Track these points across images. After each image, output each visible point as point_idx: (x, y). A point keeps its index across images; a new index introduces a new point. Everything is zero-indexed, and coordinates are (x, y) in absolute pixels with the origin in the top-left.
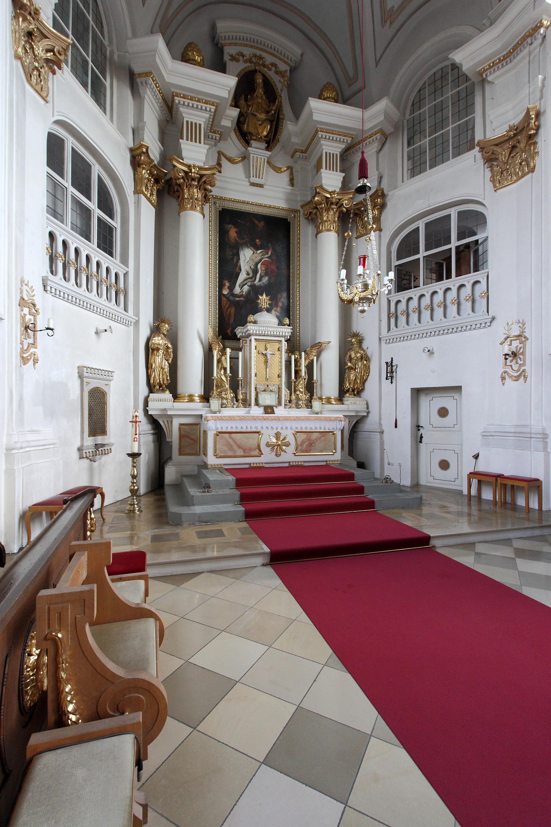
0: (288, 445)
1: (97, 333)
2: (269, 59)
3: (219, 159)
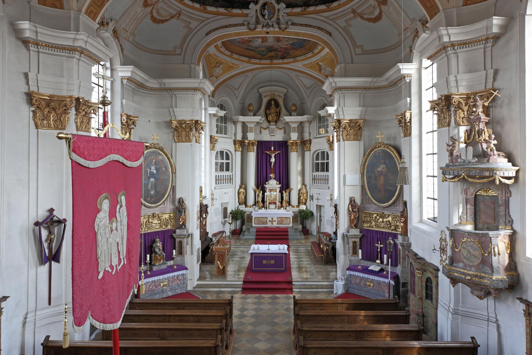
0: (275, 221)
1: (225, 193)
2: (277, 93)
3: (261, 129)
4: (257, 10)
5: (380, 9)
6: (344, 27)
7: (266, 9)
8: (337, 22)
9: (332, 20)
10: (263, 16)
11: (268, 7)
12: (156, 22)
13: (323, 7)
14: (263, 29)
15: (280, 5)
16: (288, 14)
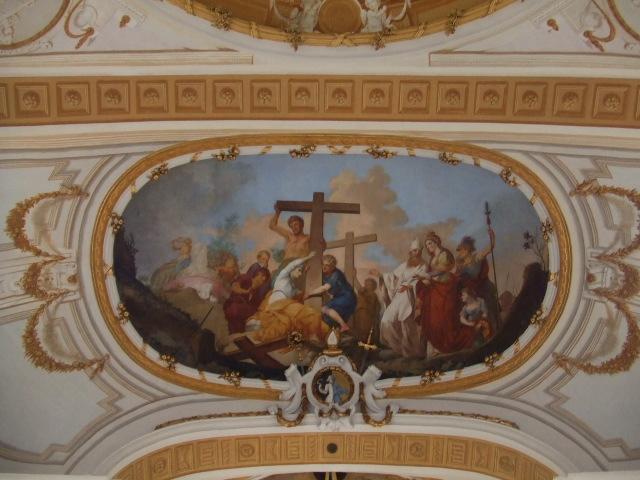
4: (304, 386)
5: (628, 316)
6: (549, 405)
7: (328, 383)
8: (522, 397)
9: (508, 396)
10: (322, 397)
11: (334, 380)
12: (34, 356)
13: (479, 369)
14: (319, 424)
15: (366, 374)
16: (390, 393)
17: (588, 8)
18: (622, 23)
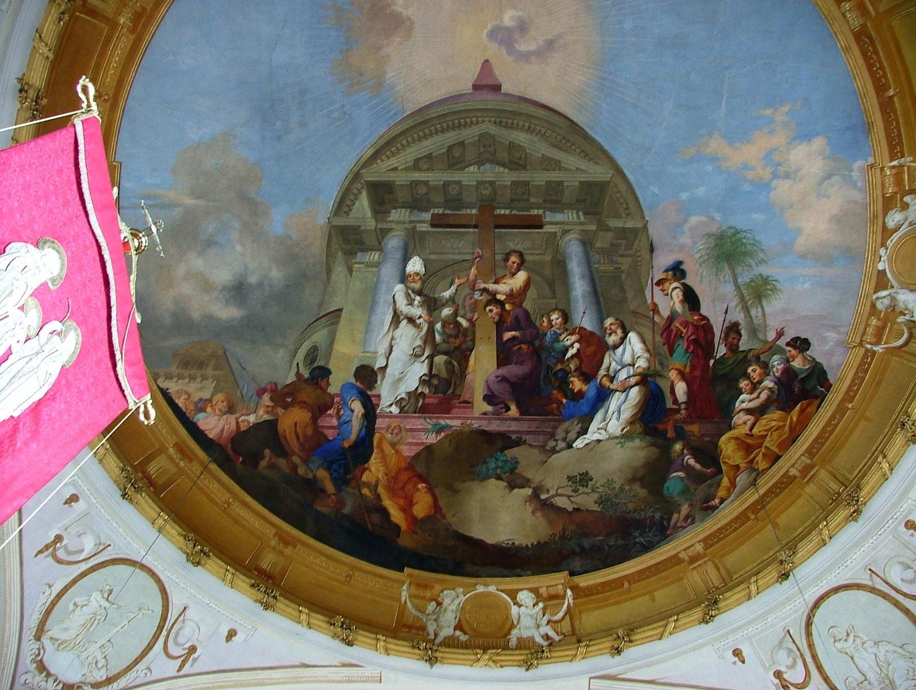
17: (781, 642)
18: (819, 668)
